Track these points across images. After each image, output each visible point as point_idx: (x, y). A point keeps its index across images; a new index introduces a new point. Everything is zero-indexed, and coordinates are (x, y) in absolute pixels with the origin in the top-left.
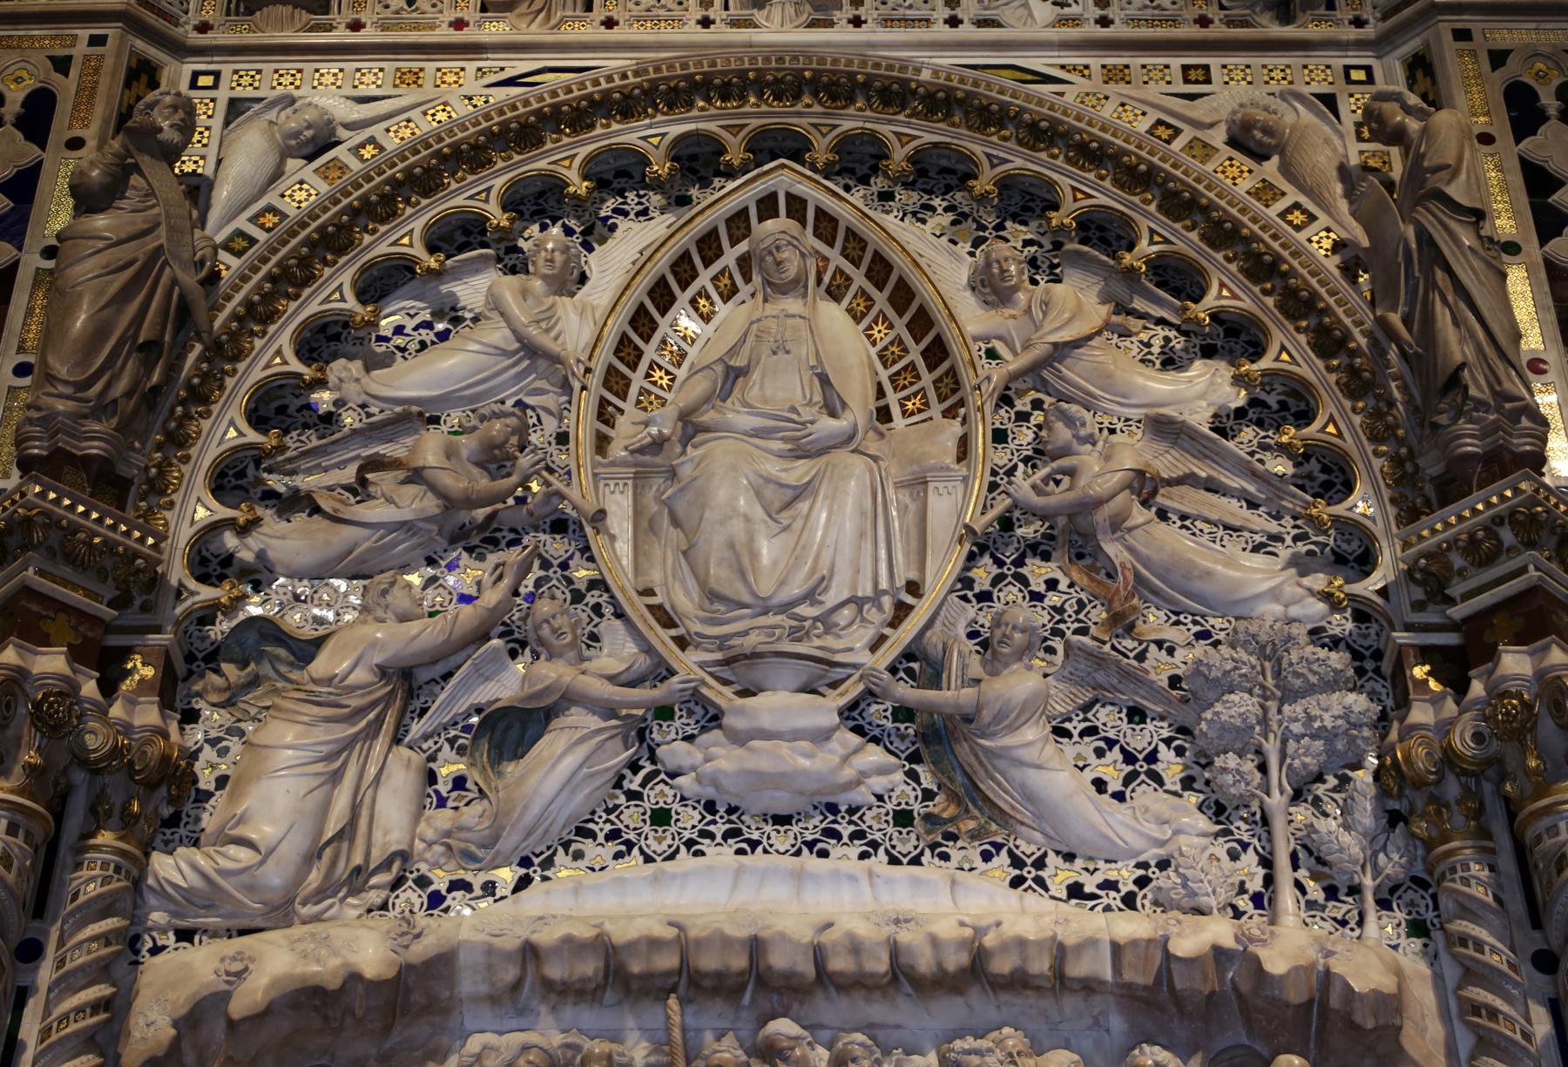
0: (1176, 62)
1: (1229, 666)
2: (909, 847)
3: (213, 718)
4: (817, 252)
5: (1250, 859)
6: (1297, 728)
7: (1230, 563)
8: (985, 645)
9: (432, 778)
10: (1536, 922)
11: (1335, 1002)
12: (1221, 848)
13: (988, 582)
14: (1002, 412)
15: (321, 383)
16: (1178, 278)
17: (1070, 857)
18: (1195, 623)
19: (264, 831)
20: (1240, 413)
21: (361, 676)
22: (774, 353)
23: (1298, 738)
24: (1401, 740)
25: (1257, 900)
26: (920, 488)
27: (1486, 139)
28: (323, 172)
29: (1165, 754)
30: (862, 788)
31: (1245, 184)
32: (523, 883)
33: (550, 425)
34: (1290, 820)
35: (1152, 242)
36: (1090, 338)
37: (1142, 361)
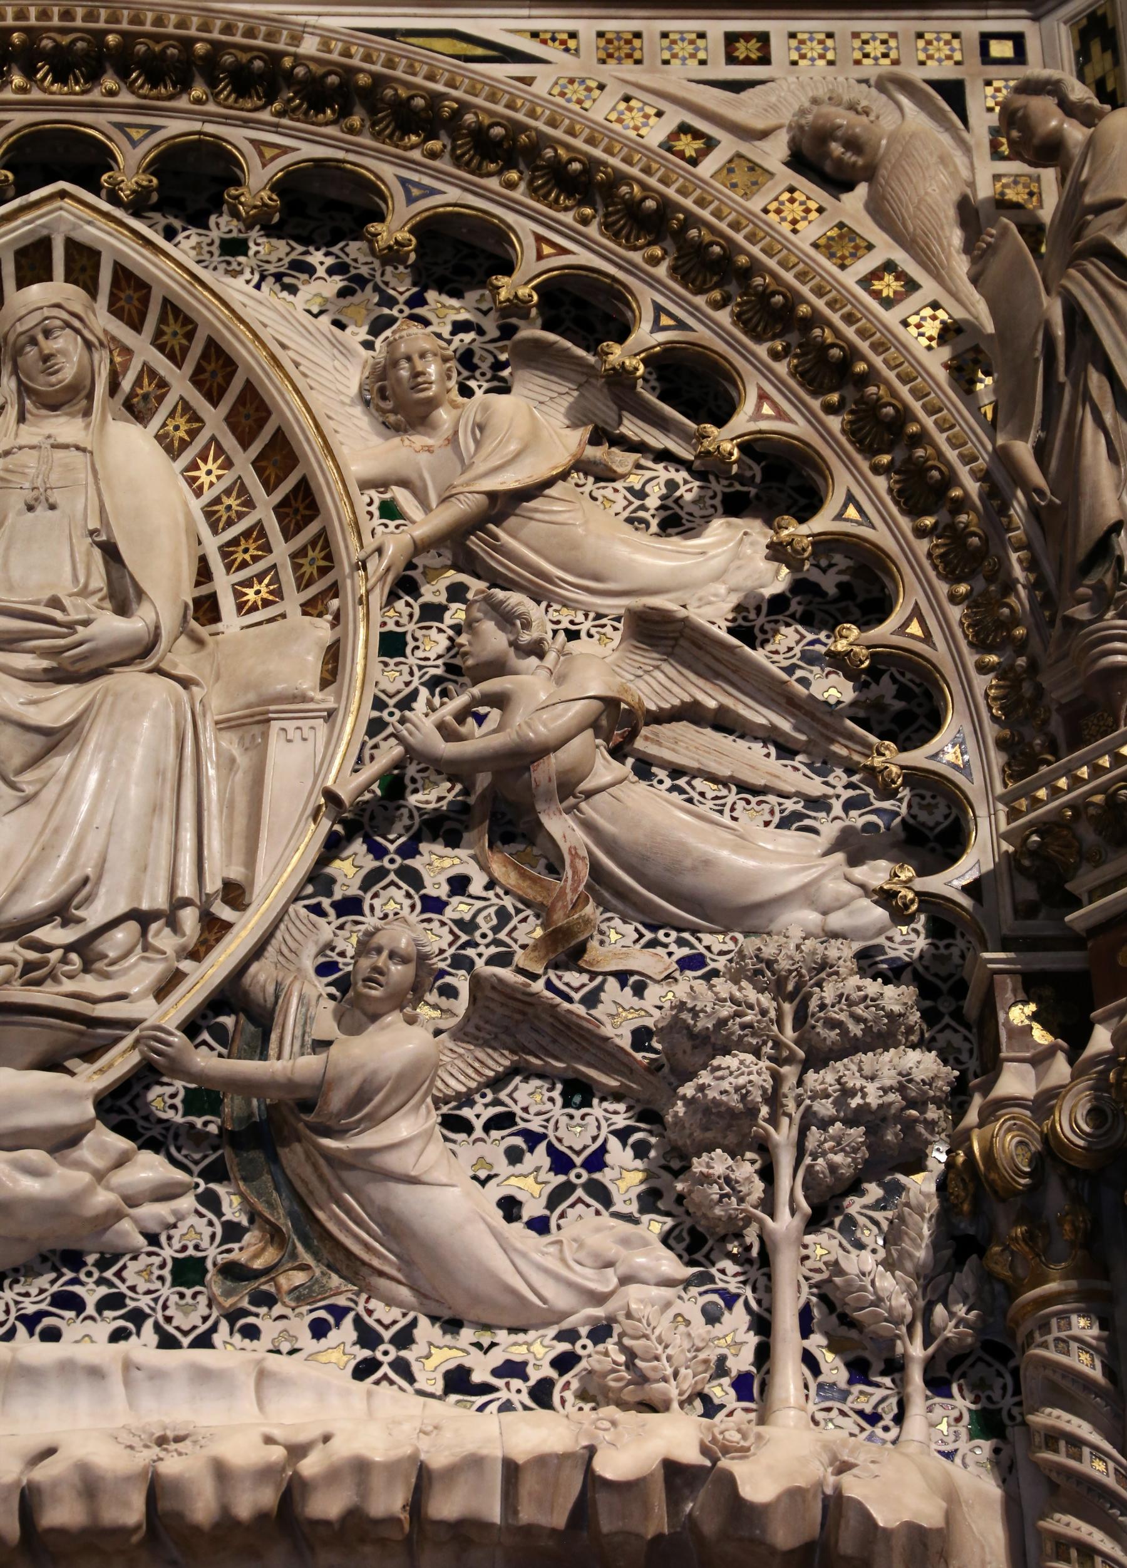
1: (726, 1011)
2: (195, 1319)
4: (114, 339)
5: (737, 1320)
6: (825, 1108)
7: (743, 843)
8: (344, 984)
12: (692, 1305)
13: (357, 882)
14: (400, 605)
16: (694, 384)
17: (453, 1325)
18: (681, 942)
20: (778, 603)
22: (30, 508)
23: (825, 1124)
24: (981, 1125)
25: (742, 1386)
26: (256, 729)
29: (619, 1155)
30: (126, 1225)
34: (804, 1256)
35: (657, 327)
36: (549, 483)
37: (630, 520)
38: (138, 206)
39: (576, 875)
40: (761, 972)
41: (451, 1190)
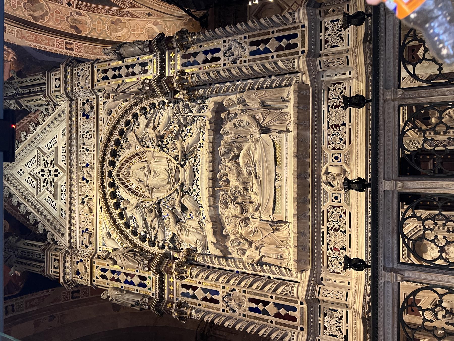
0: (99, 122)
3: (182, 246)
5: (199, 118)
7: (164, 118)
9: (190, 219)
10: (206, 85)
11: (215, 110)
15: (140, 233)
16: (128, 123)
17: (199, 140)
19: (195, 239)
20: (145, 116)
21: (177, 228)
25: (204, 118)
27: (109, 83)
28: (113, 234)
31: (115, 114)
32: (202, 207)
33: (146, 204)
34: (195, 113)
38: (114, 168)
39: (166, 132)
40: (173, 117)
41: (189, 141)
